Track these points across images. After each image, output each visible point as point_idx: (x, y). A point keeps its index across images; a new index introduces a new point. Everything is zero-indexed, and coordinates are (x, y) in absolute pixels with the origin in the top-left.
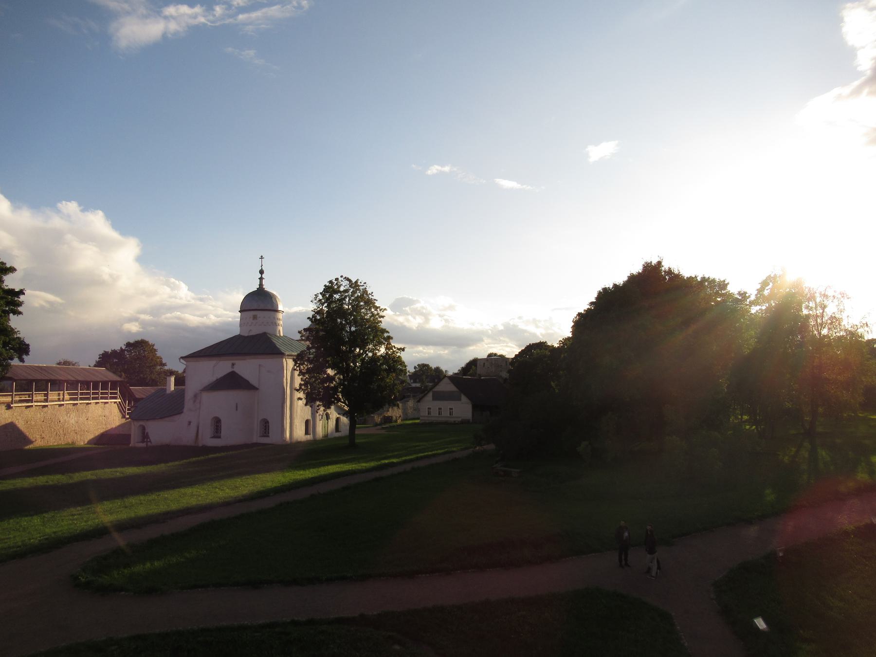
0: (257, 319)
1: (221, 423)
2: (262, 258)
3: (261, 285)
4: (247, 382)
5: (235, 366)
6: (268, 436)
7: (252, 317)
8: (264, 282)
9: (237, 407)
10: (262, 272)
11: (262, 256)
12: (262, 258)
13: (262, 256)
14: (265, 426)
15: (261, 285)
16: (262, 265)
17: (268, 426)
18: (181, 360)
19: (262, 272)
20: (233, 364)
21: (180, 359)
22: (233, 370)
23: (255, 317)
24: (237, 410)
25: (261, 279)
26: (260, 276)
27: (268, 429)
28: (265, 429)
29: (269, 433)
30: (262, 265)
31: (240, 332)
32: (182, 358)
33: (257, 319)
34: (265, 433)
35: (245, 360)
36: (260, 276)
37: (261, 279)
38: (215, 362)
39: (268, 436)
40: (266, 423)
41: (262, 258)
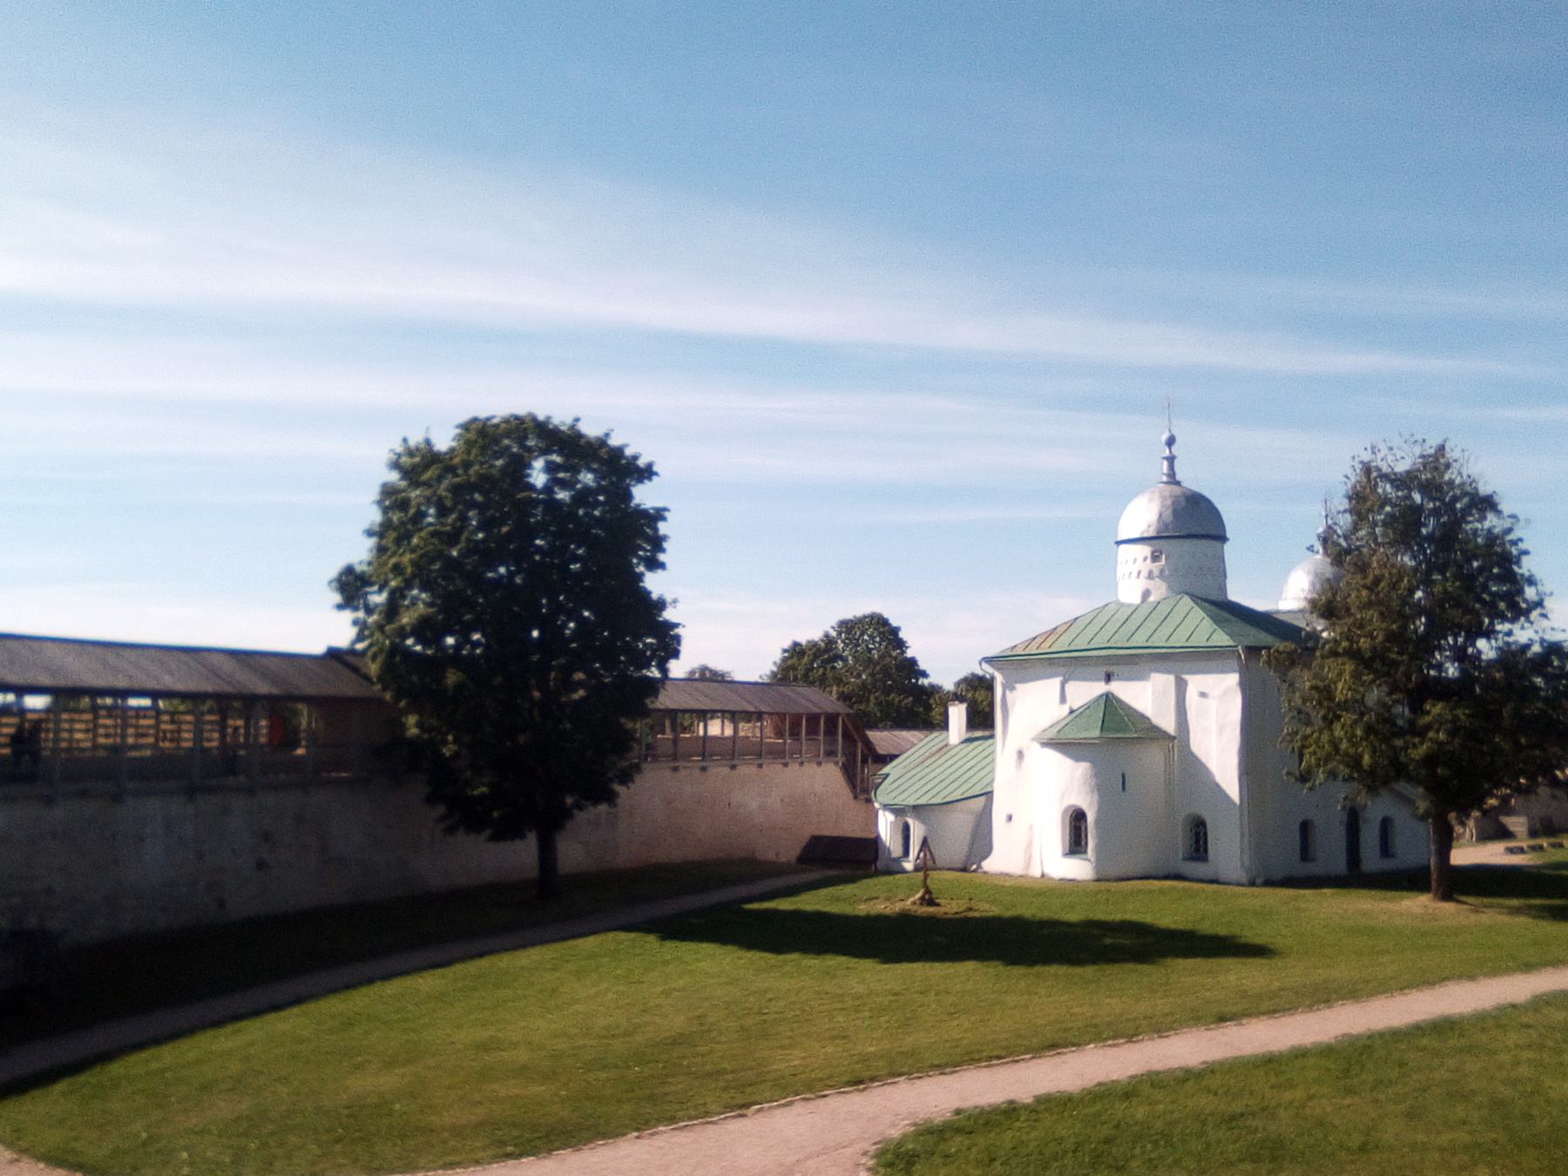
1: (1086, 821)
3: (1172, 474)
7: (1149, 555)
14: (1197, 834)
17: (1205, 834)
19: (1171, 442)
25: (1171, 460)
27: (1206, 842)
28: (1197, 842)
29: (1206, 851)
34: (1197, 850)
37: (1171, 460)
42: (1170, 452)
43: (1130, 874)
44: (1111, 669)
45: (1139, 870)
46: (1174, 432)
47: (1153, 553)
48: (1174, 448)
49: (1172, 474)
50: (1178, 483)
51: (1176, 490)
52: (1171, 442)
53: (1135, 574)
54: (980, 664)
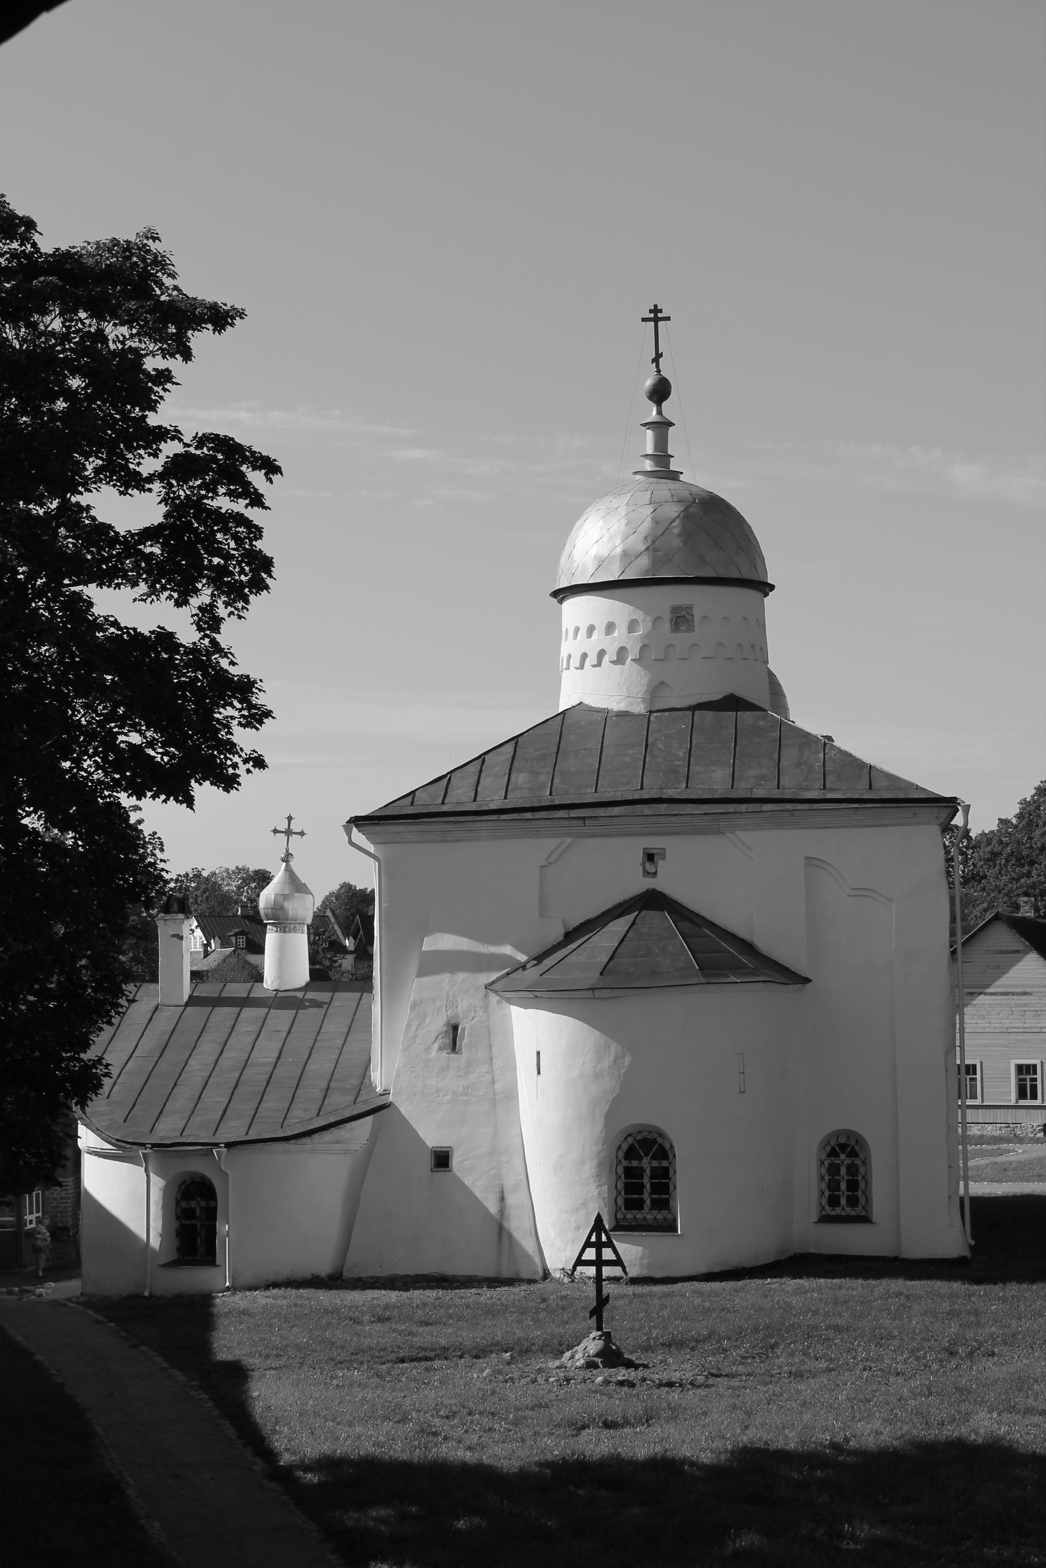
0: (691, 628)
3: (662, 457)
4: (748, 947)
5: (663, 866)
6: (865, 1219)
7: (667, 616)
11: (656, 310)
12: (656, 320)
13: (656, 310)
14: (833, 1169)
16: (658, 356)
17: (853, 1170)
18: (357, 836)
19: (660, 392)
20: (650, 857)
22: (648, 884)
23: (681, 619)
27: (853, 1185)
28: (833, 1186)
29: (853, 1202)
30: (658, 356)
32: (357, 821)
33: (691, 628)
34: (834, 1201)
35: (720, 832)
37: (662, 427)
38: (557, 841)
39: (865, 1219)
40: (833, 1153)
41: (656, 316)
42: (660, 412)
43: (749, 1262)
44: (653, 843)
45: (765, 1251)
47: (675, 610)
49: (662, 457)
50: (674, 476)
51: (665, 487)
52: (660, 392)
53: (611, 655)
54: (349, 833)
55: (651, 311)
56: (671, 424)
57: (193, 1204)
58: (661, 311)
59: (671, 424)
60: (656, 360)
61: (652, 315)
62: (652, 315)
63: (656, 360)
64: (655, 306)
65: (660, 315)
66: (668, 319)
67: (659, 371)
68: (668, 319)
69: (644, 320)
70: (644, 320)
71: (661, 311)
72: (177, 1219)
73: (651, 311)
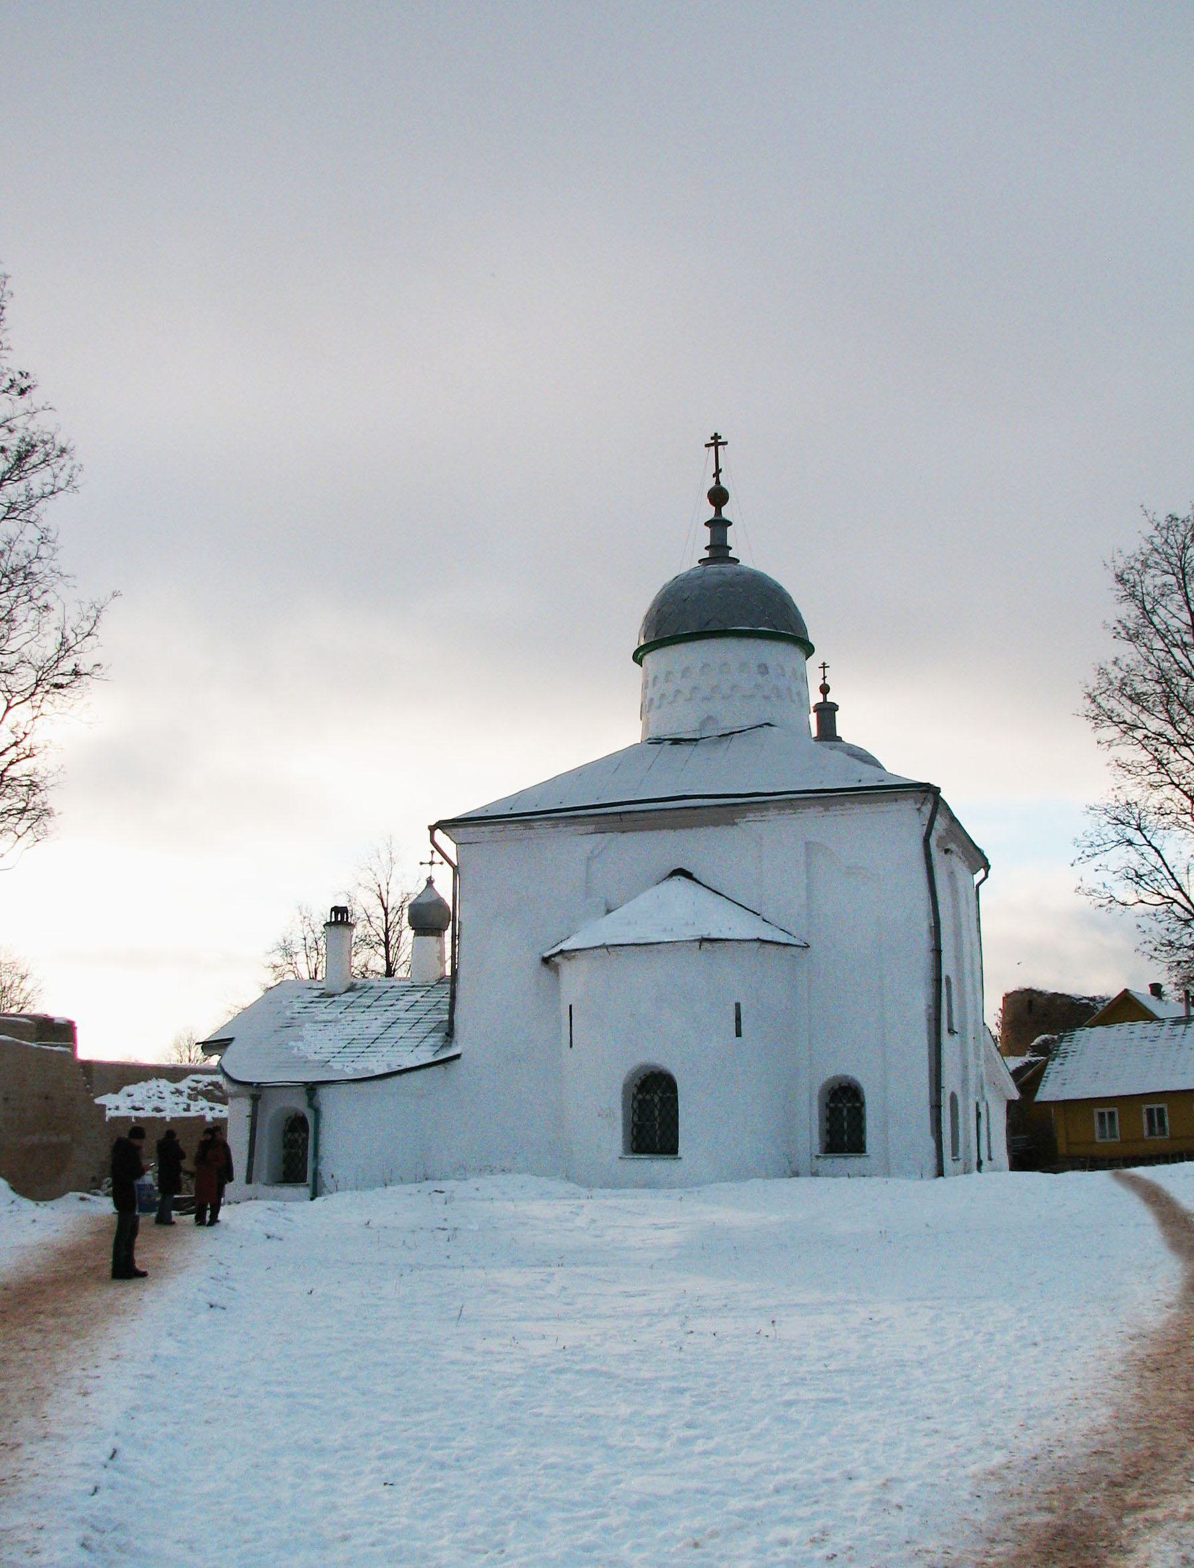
2: (716, 442)
3: (719, 550)
8: (733, 537)
9: (738, 1019)
10: (718, 497)
11: (716, 437)
13: (716, 437)
15: (719, 550)
16: (718, 471)
19: (718, 497)
21: (432, 829)
24: (739, 1034)
25: (718, 525)
26: (710, 512)
30: (718, 471)
31: (646, 727)
32: (442, 825)
36: (710, 512)
37: (718, 525)
41: (716, 442)
46: (723, 484)
48: (726, 512)
55: (712, 438)
56: (730, 524)
57: (296, 1135)
58: (720, 437)
59: (730, 524)
60: (717, 474)
61: (713, 441)
62: (713, 441)
63: (717, 474)
64: (716, 434)
65: (719, 441)
66: (725, 443)
67: (718, 482)
68: (725, 443)
69: (707, 446)
70: (707, 446)
71: (720, 437)
72: (285, 1147)
73: (712, 438)
